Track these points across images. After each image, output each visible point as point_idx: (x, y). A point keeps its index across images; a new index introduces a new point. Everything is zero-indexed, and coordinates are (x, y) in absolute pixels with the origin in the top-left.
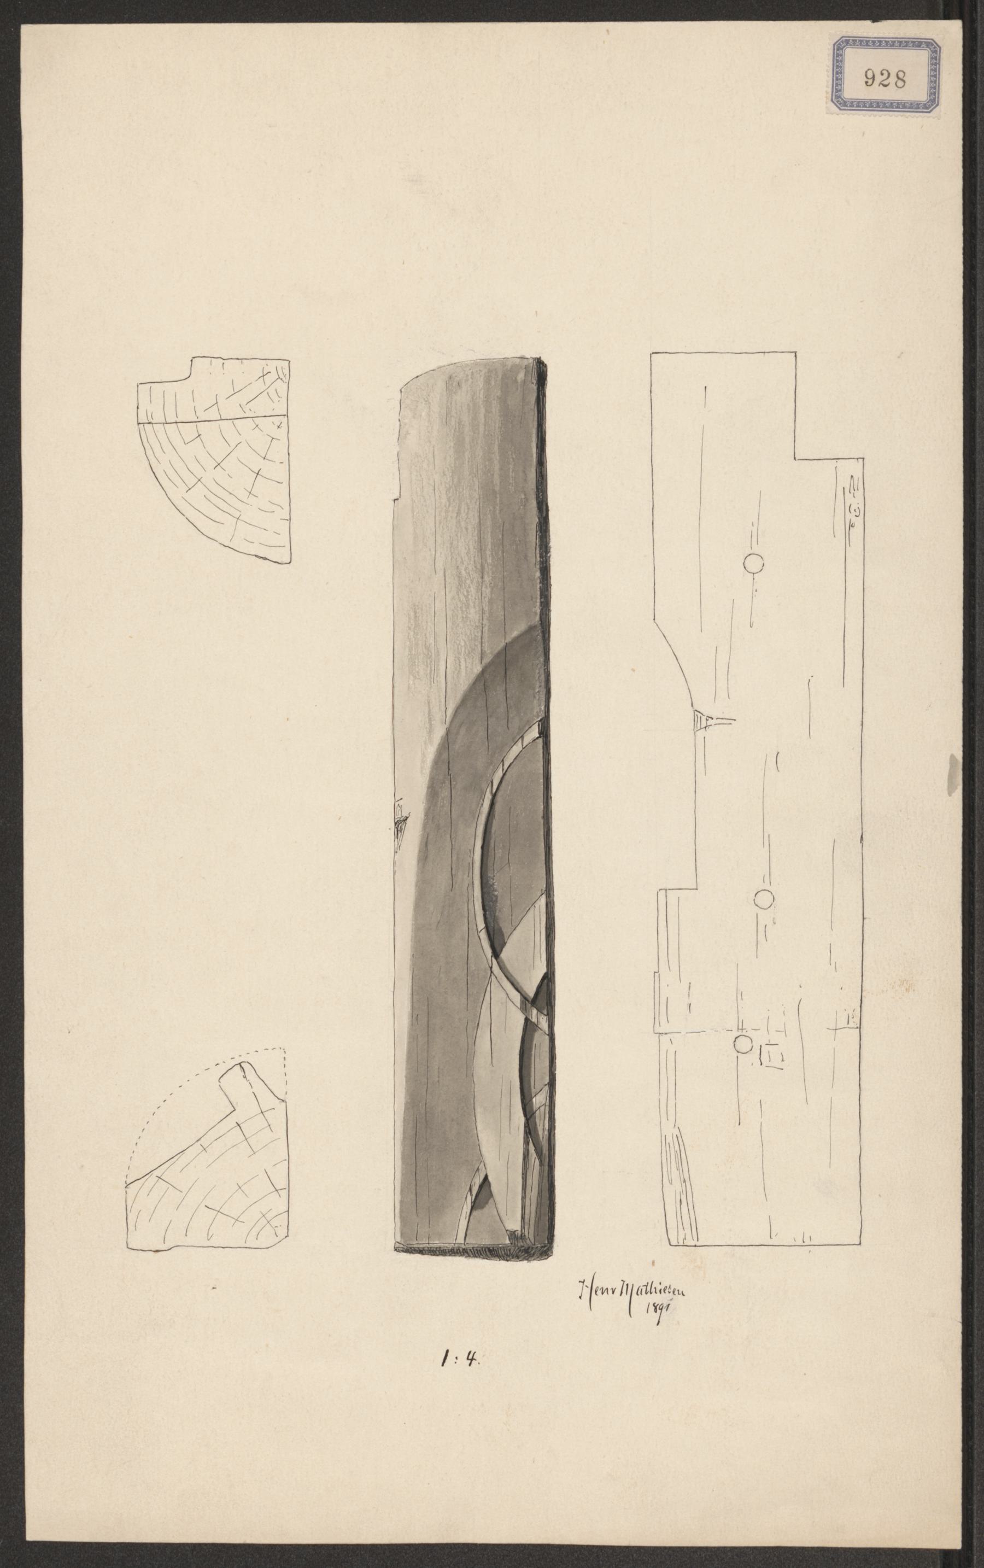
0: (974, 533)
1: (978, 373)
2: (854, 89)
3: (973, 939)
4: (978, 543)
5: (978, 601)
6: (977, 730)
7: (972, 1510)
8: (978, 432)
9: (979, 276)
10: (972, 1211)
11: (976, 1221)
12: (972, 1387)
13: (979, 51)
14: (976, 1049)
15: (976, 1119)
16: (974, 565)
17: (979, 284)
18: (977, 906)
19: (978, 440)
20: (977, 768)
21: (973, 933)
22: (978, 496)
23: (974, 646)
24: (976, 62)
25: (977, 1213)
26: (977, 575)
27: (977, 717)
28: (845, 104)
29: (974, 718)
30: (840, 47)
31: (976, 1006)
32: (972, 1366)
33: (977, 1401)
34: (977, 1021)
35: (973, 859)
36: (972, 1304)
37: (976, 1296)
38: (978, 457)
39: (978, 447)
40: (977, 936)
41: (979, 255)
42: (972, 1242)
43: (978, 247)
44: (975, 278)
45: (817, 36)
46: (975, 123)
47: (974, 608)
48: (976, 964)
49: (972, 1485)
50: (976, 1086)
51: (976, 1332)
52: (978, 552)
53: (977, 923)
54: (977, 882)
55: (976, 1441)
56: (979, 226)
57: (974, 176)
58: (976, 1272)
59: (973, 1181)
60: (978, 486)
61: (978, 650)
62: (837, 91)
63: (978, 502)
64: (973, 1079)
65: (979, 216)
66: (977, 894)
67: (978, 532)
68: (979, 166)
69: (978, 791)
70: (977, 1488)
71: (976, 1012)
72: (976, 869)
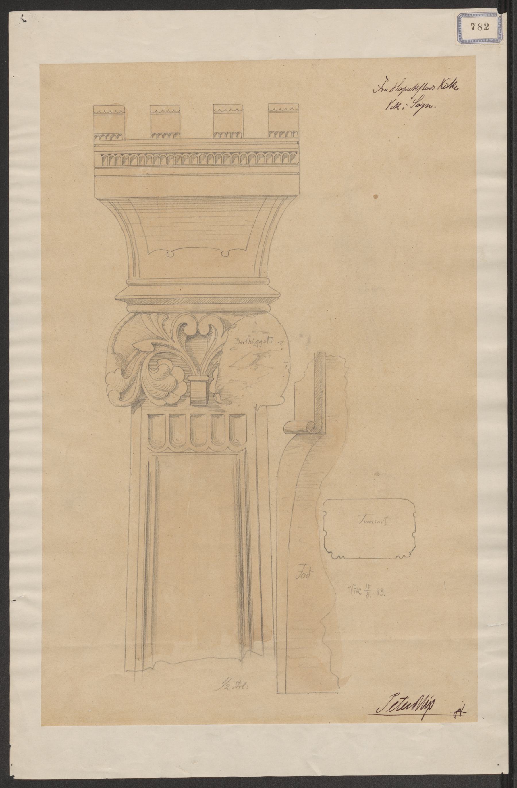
0: (512, 267)
1: (514, 199)
2: (468, 33)
3: (512, 437)
4: (513, 271)
5: (514, 295)
6: (513, 349)
7: (512, 677)
8: (513, 224)
9: (514, 158)
11: (514, 556)
12: (512, 626)
13: (514, 63)
14: (514, 484)
15: (514, 513)
16: (512, 280)
17: (514, 162)
18: (514, 424)
19: (514, 227)
20: (514, 365)
21: (512, 435)
22: (514, 251)
24: (512, 68)
26: (513, 284)
27: (514, 344)
28: (463, 41)
29: (512, 344)
30: (459, 18)
31: (514, 465)
32: (512, 617)
33: (514, 632)
34: (514, 472)
36: (512, 591)
37: (514, 587)
39: (514, 230)
41: (514, 149)
42: (512, 565)
43: (513, 146)
44: (512, 159)
45: (449, 15)
46: (512, 94)
47: (512, 298)
48: (514, 448)
49: (512, 668)
50: (514, 499)
51: (514, 603)
52: (514, 274)
54: (514, 413)
55: (514, 649)
56: (514, 137)
57: (512, 116)
58: (514, 577)
59: (512, 539)
60: (513, 247)
61: (514, 315)
62: (460, 36)
63: (513, 253)
64: (512, 496)
65: (513, 133)
66: (514, 419)
67: (513, 266)
68: (513, 112)
69: (514, 375)
71: (514, 468)
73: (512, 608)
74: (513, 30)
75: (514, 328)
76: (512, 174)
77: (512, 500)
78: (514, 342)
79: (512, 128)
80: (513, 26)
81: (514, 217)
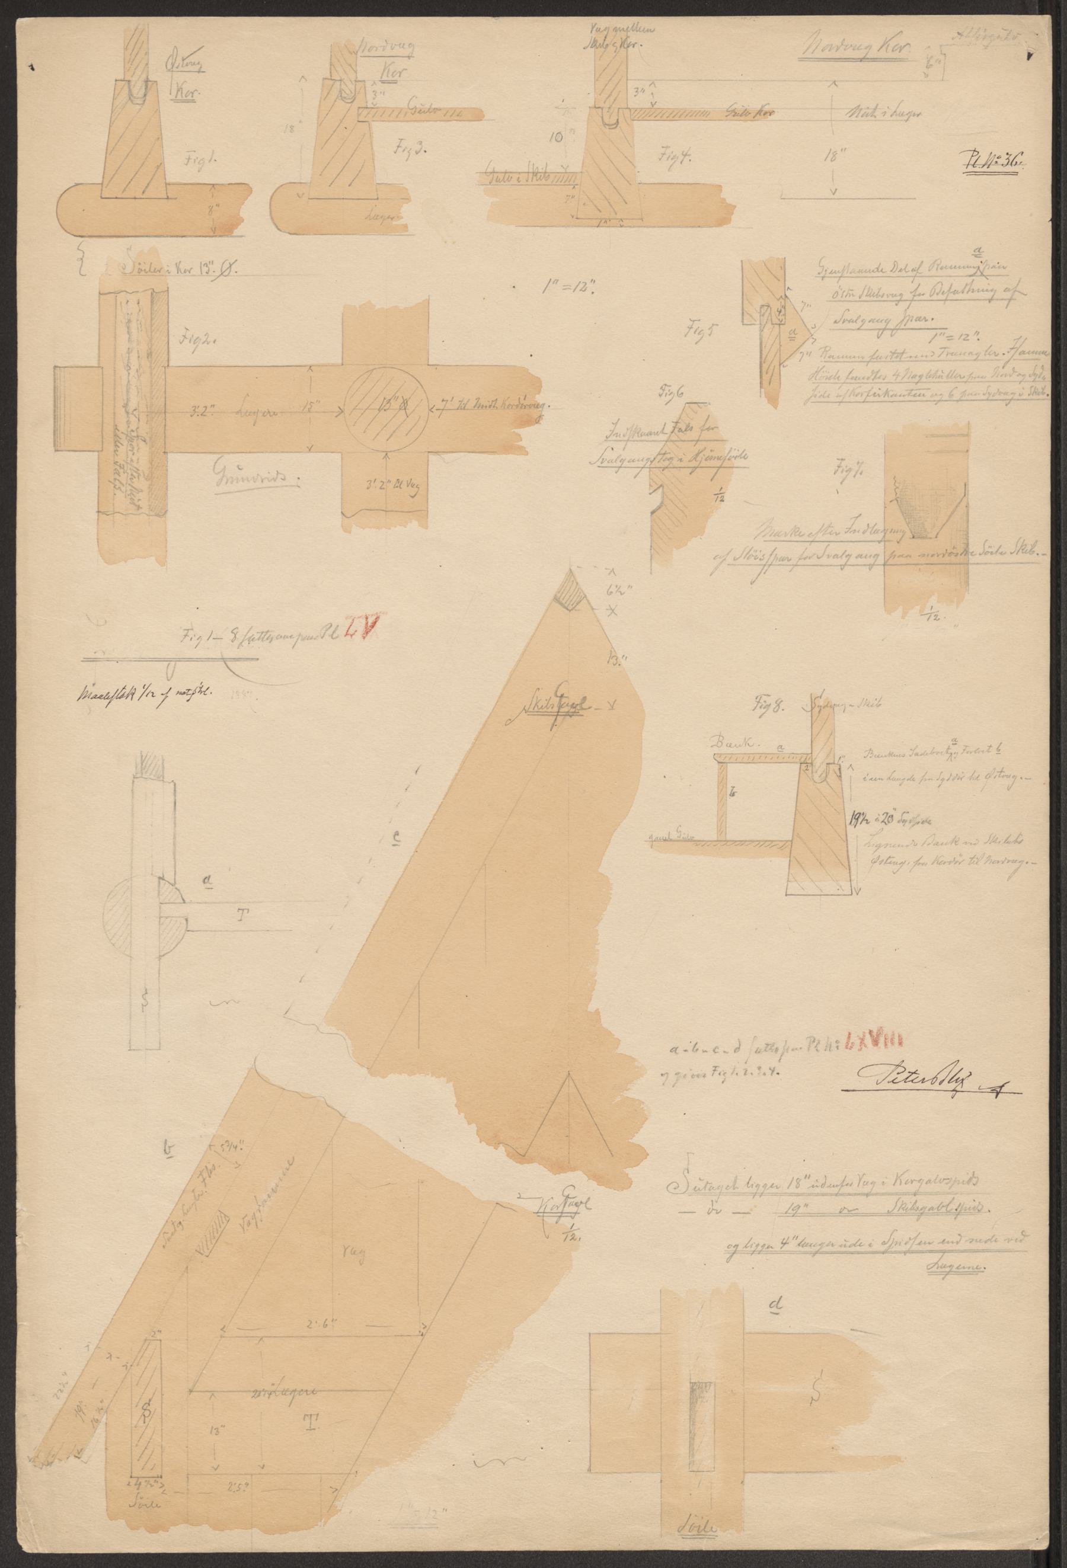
9: (1063, 592)
11: (1063, 1281)
13: (1062, 427)
17: (1063, 597)
19: (1063, 711)
20: (1063, 951)
22: (1062, 752)
25: (1063, 1275)
35: (1059, 1017)
39: (1063, 715)
40: (1062, 1072)
41: (1063, 576)
53: (1062, 1063)
67: (1063, 778)
72: (1062, 1025)
73: (1059, 1371)
74: (1062, 370)
75: (1062, 886)
78: (1063, 909)
79: (1059, 540)
80: (1062, 362)
81: (1063, 693)
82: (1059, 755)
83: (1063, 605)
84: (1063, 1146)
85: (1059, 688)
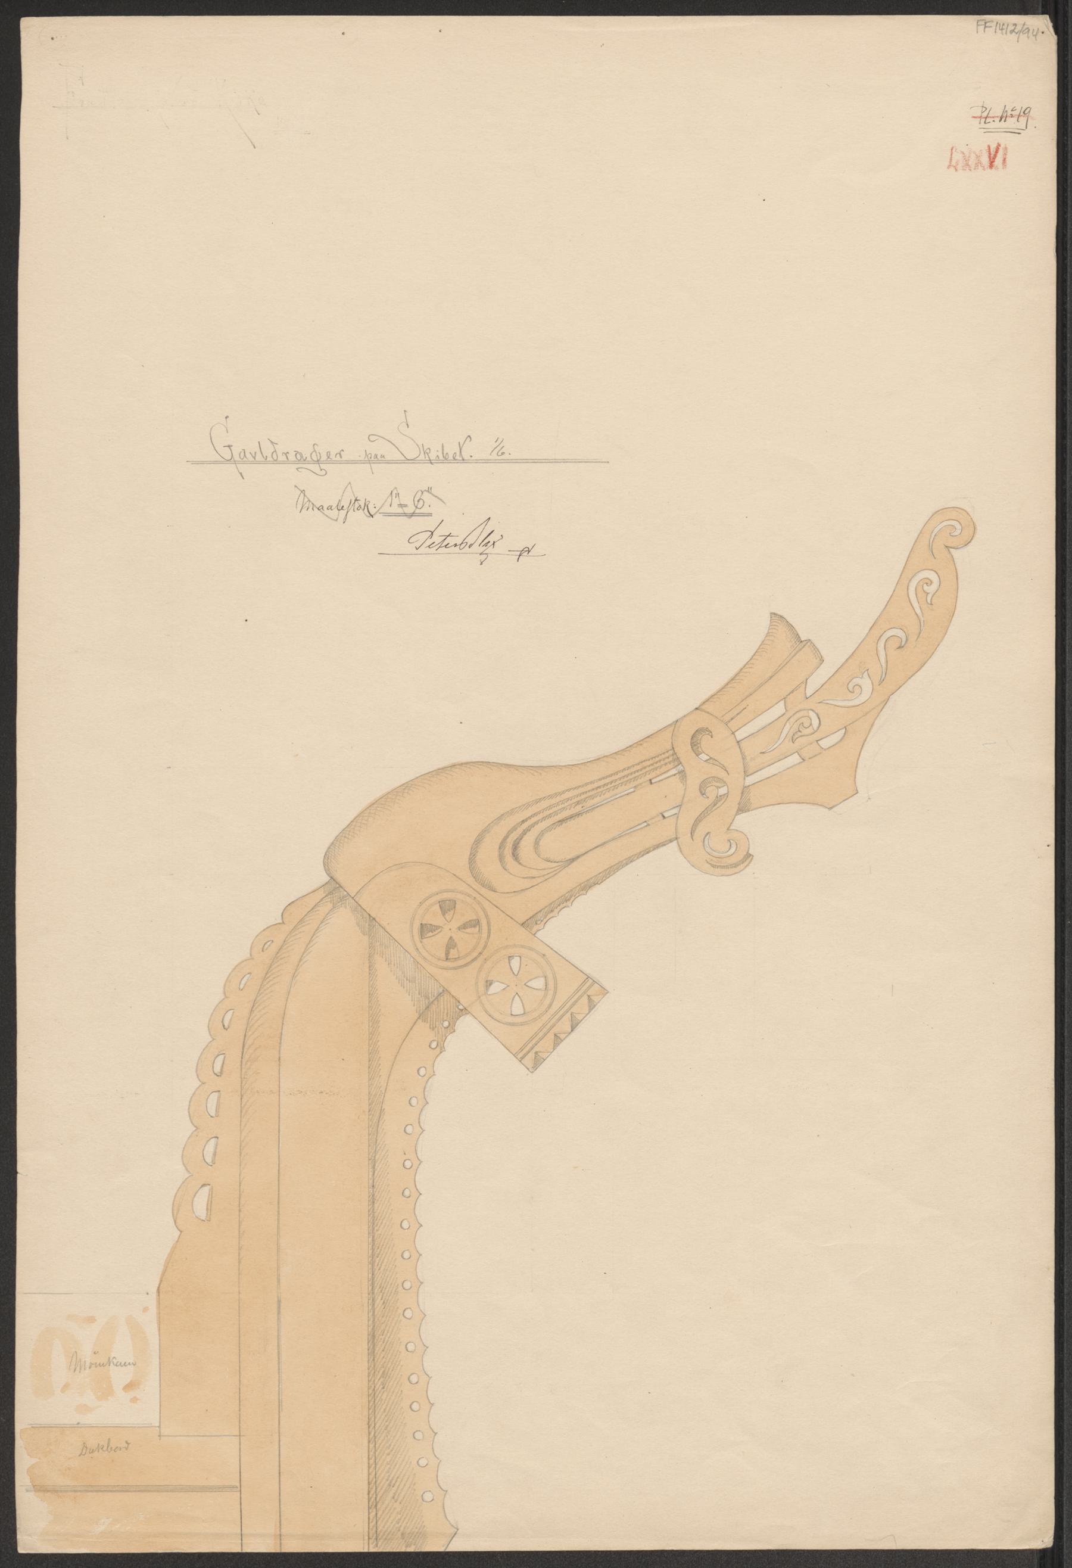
10: (1063, 1283)
11: (1066, 1291)
12: (1062, 1411)
13: (1068, 436)
17: (1068, 607)
19: (1068, 720)
22: (1067, 761)
23: (1064, 872)
38: (1068, 733)
39: (1068, 725)
41: (1068, 586)
43: (1068, 580)
58: (1066, 1327)
63: (1067, 765)
68: (1068, 521)
69: (1067, 977)
70: (1066, 1485)
76: (1064, 629)
77: (1063, 1194)
81: (1068, 702)
82: (1064, 764)
83: (1068, 615)
84: (1066, 1156)
85: (1064, 697)
